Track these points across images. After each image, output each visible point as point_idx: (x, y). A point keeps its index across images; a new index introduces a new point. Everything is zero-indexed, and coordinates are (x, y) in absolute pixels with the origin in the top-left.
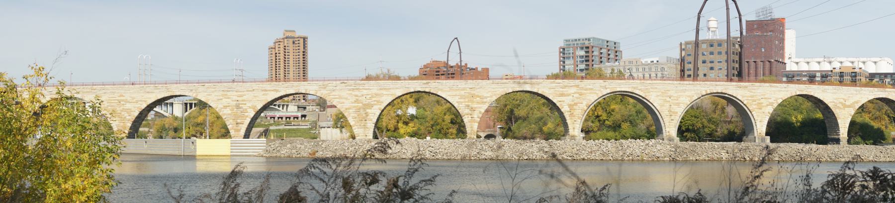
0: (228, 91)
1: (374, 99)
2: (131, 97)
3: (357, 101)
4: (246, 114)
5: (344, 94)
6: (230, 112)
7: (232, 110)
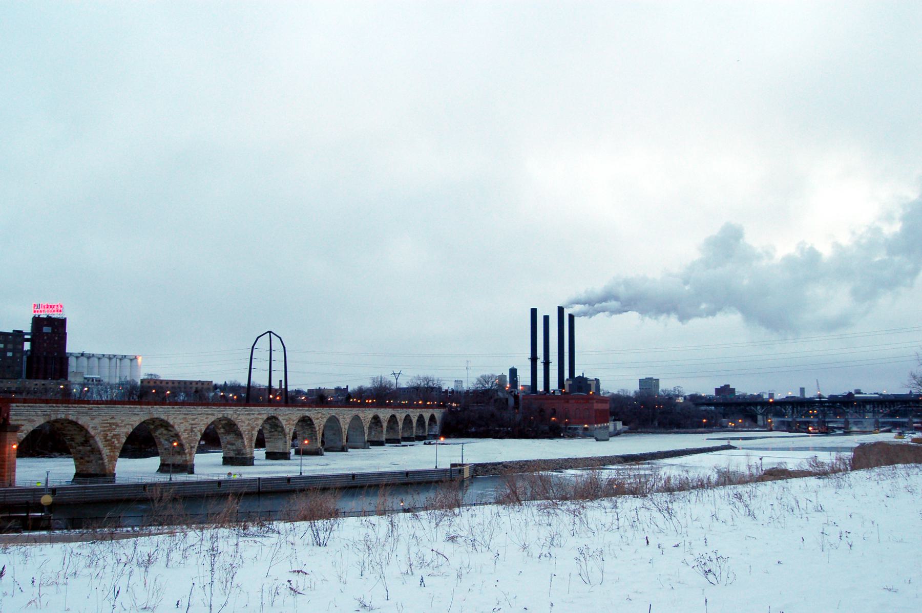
0: (188, 414)
1: (255, 422)
2: (120, 420)
3: (249, 424)
4: (197, 438)
5: (243, 418)
6: (187, 436)
7: (188, 434)
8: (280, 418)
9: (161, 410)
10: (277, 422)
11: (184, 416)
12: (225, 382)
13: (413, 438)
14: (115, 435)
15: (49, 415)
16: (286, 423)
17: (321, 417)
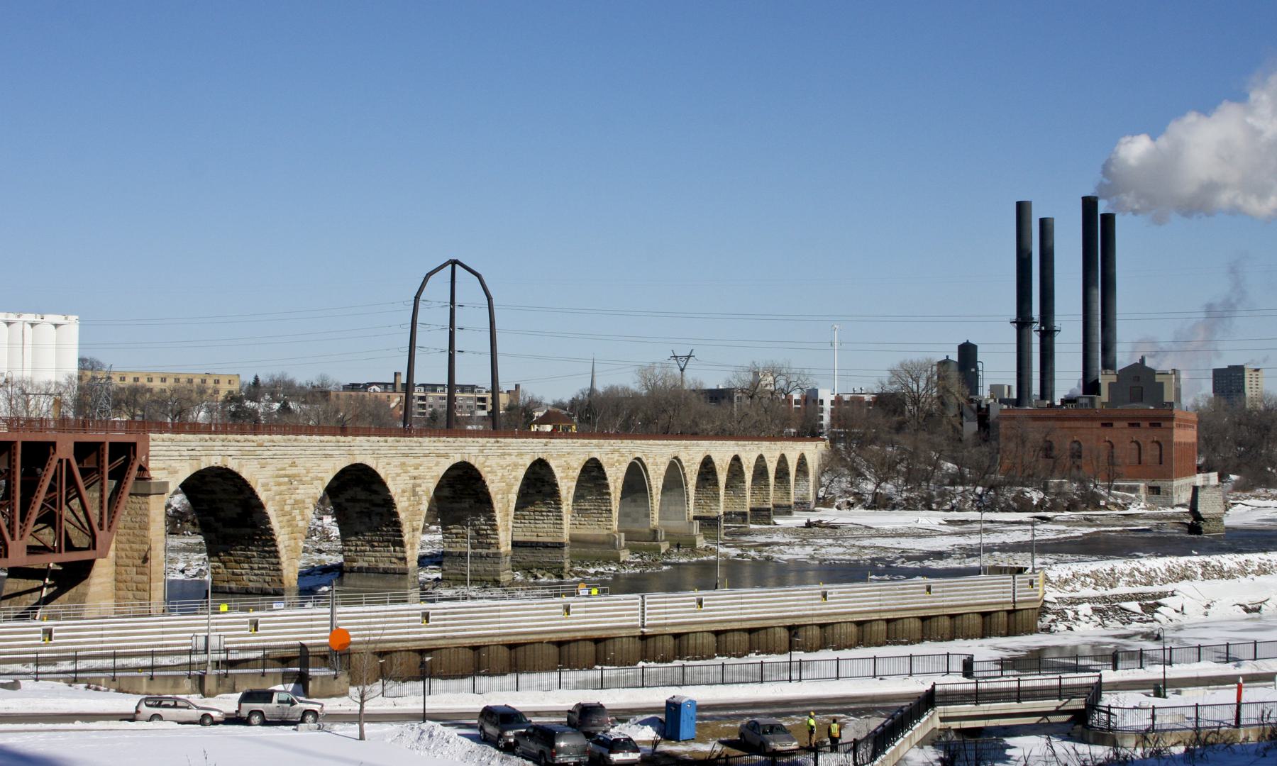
8: (553, 464)
9: (366, 446)
10: (543, 472)
11: (403, 460)
12: (256, 379)
13: (769, 510)
14: (296, 502)
15: (197, 458)
16: (562, 475)
17: (618, 461)
